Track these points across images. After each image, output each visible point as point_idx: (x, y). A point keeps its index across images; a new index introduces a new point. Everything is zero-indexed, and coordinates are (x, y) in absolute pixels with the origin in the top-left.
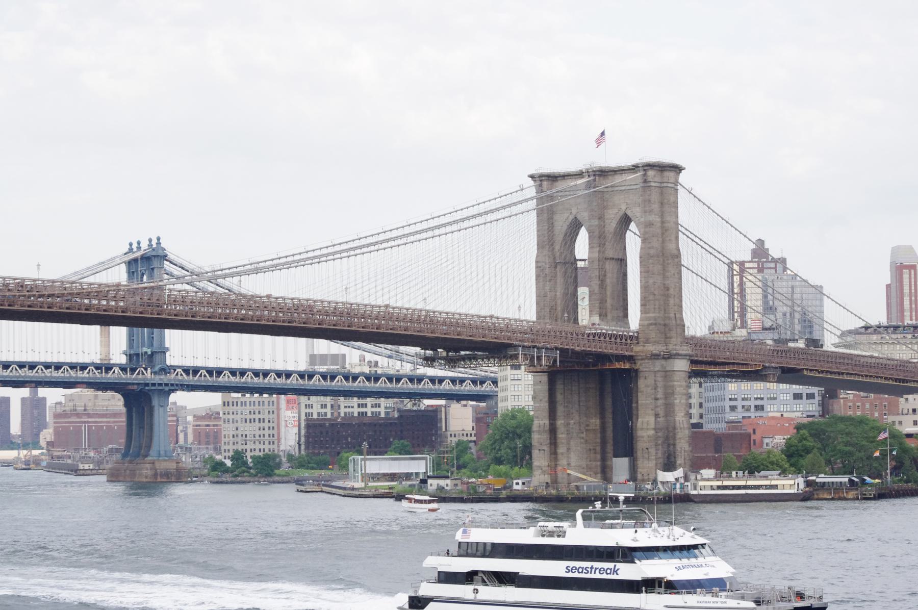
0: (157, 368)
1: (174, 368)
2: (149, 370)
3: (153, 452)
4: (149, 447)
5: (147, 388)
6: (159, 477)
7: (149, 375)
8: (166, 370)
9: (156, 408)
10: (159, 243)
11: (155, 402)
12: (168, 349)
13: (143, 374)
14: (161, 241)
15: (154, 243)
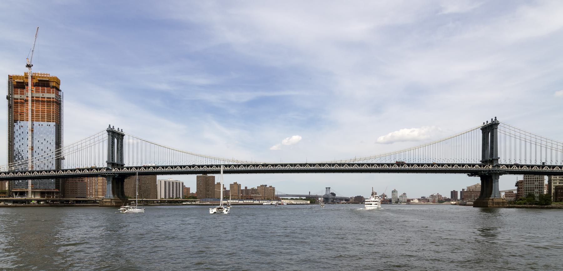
0: (495, 164)
1: (502, 165)
2: (491, 166)
3: (493, 195)
4: (491, 193)
5: (490, 172)
6: (494, 205)
7: (491, 167)
8: (498, 166)
9: (494, 180)
10: (496, 119)
11: (493, 178)
12: (499, 158)
13: (488, 167)
14: (497, 118)
15: (494, 120)
